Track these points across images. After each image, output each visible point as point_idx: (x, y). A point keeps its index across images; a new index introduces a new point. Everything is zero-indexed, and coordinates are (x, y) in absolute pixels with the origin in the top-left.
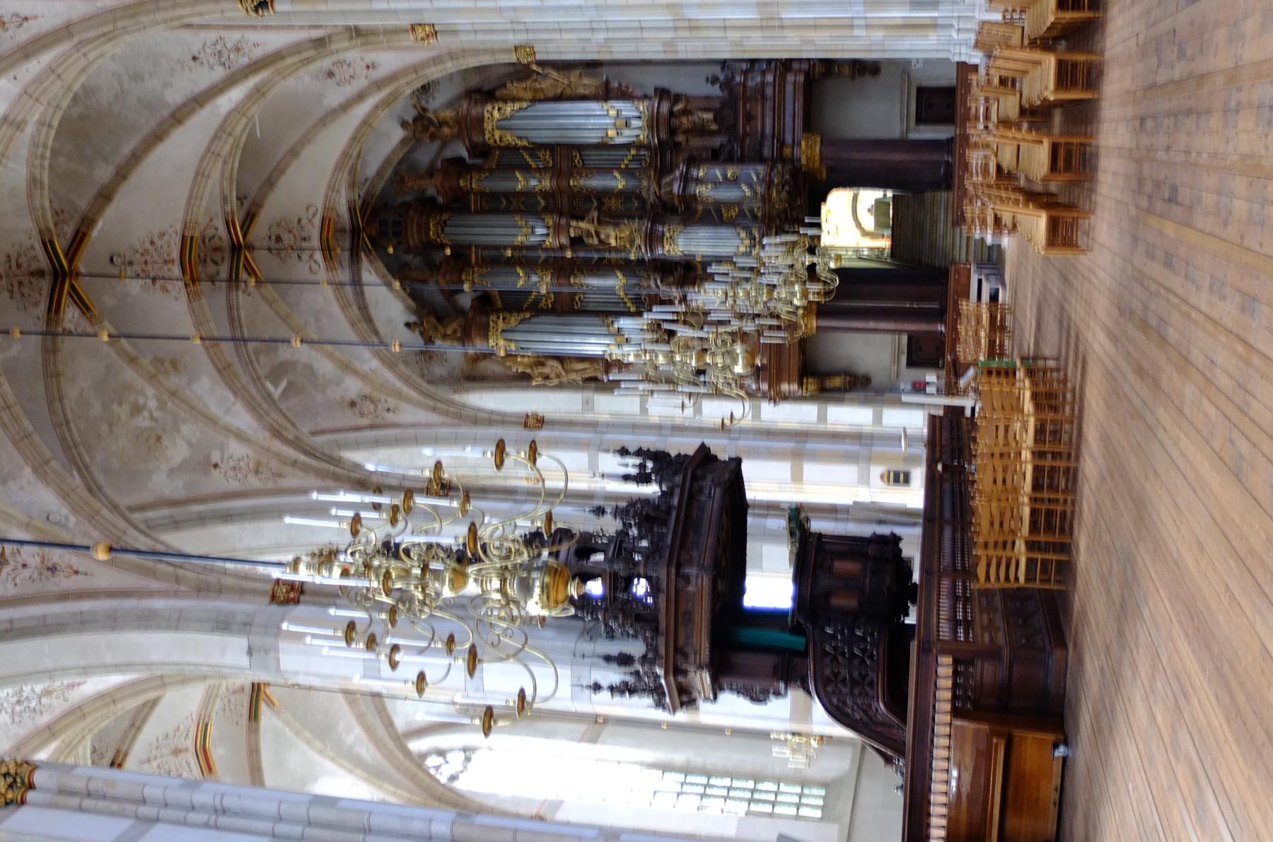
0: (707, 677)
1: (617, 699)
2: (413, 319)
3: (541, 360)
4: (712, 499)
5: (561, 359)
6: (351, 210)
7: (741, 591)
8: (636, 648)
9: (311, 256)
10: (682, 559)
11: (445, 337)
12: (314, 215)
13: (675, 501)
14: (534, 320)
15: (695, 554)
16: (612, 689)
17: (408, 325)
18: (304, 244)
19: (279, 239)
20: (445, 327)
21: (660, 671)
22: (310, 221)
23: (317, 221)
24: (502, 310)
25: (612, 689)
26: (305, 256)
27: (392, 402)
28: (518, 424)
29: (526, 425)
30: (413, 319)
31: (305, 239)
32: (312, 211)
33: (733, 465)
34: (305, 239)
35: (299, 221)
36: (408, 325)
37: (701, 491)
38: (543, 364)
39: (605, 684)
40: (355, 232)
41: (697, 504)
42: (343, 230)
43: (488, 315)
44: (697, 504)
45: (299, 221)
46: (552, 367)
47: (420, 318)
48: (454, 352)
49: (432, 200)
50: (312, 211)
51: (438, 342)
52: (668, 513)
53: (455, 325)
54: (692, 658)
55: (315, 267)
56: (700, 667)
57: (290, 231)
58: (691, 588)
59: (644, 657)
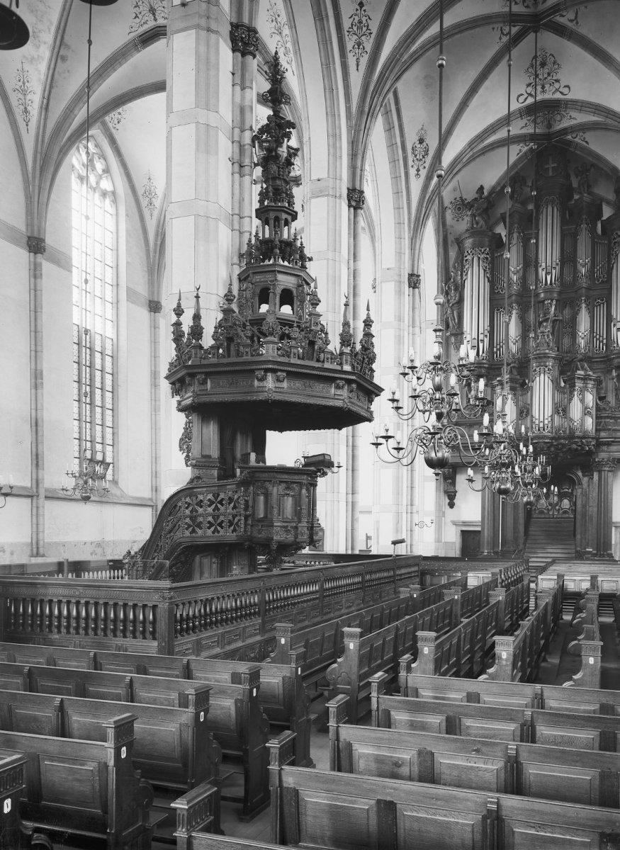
0: (189, 401)
1: (172, 329)
2: (486, 193)
3: (460, 288)
4: (339, 397)
5: (461, 301)
6: (565, 131)
7: (281, 428)
8: (207, 341)
9: (530, 95)
10: (279, 373)
11: (473, 216)
12: (562, 93)
13: (327, 365)
14: (486, 279)
15: (285, 385)
16: (178, 325)
17: (482, 188)
18: (539, 88)
19: (543, 65)
20: (479, 215)
21: (190, 363)
22: (557, 90)
23: (558, 96)
24: (492, 258)
25: (178, 325)
26: (530, 90)
27: (423, 173)
28: (413, 271)
29: (411, 275)
30: (486, 193)
31: (543, 87)
32: (566, 91)
33: (363, 413)
34: (543, 87)
35: (557, 81)
36: (482, 188)
37: (338, 387)
38: (455, 290)
39: (182, 319)
40: (548, 136)
41: (338, 389)
42: (549, 126)
43: (490, 246)
44: (338, 389)
45: (557, 81)
46: (454, 297)
47: (487, 198)
48: (462, 225)
49: (571, 197)
50: (566, 91)
51: (469, 213)
52: (318, 361)
53: (482, 222)
54: (203, 387)
55: (521, 99)
56: (196, 395)
57: (549, 74)
58: (256, 383)
59: (201, 347)
